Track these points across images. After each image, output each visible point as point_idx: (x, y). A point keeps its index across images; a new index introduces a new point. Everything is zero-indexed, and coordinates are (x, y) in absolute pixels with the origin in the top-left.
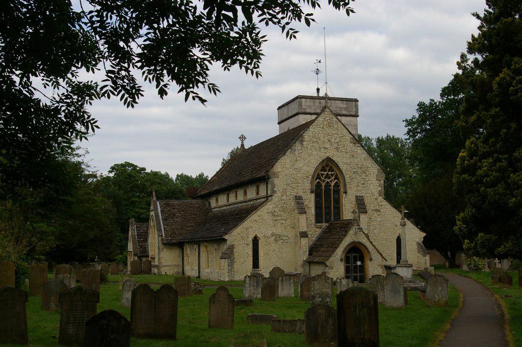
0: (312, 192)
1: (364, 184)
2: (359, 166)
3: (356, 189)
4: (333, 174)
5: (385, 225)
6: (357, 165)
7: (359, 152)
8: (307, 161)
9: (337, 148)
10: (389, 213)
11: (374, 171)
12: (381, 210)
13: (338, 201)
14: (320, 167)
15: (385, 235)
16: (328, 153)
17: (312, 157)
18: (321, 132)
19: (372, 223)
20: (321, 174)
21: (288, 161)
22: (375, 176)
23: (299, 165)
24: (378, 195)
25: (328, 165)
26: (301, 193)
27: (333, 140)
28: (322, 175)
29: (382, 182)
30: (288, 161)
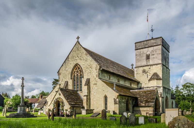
0: (71, 79)
1: (90, 73)
2: (89, 65)
3: (87, 75)
7: (89, 58)
8: (70, 67)
9: (80, 59)
10: (100, 85)
12: (97, 84)
13: (81, 82)
15: (99, 95)
16: (77, 62)
17: (71, 65)
21: (64, 68)
23: (67, 69)
24: (96, 77)
25: (77, 66)
26: (68, 80)
27: (79, 56)
28: (76, 71)
29: (98, 70)
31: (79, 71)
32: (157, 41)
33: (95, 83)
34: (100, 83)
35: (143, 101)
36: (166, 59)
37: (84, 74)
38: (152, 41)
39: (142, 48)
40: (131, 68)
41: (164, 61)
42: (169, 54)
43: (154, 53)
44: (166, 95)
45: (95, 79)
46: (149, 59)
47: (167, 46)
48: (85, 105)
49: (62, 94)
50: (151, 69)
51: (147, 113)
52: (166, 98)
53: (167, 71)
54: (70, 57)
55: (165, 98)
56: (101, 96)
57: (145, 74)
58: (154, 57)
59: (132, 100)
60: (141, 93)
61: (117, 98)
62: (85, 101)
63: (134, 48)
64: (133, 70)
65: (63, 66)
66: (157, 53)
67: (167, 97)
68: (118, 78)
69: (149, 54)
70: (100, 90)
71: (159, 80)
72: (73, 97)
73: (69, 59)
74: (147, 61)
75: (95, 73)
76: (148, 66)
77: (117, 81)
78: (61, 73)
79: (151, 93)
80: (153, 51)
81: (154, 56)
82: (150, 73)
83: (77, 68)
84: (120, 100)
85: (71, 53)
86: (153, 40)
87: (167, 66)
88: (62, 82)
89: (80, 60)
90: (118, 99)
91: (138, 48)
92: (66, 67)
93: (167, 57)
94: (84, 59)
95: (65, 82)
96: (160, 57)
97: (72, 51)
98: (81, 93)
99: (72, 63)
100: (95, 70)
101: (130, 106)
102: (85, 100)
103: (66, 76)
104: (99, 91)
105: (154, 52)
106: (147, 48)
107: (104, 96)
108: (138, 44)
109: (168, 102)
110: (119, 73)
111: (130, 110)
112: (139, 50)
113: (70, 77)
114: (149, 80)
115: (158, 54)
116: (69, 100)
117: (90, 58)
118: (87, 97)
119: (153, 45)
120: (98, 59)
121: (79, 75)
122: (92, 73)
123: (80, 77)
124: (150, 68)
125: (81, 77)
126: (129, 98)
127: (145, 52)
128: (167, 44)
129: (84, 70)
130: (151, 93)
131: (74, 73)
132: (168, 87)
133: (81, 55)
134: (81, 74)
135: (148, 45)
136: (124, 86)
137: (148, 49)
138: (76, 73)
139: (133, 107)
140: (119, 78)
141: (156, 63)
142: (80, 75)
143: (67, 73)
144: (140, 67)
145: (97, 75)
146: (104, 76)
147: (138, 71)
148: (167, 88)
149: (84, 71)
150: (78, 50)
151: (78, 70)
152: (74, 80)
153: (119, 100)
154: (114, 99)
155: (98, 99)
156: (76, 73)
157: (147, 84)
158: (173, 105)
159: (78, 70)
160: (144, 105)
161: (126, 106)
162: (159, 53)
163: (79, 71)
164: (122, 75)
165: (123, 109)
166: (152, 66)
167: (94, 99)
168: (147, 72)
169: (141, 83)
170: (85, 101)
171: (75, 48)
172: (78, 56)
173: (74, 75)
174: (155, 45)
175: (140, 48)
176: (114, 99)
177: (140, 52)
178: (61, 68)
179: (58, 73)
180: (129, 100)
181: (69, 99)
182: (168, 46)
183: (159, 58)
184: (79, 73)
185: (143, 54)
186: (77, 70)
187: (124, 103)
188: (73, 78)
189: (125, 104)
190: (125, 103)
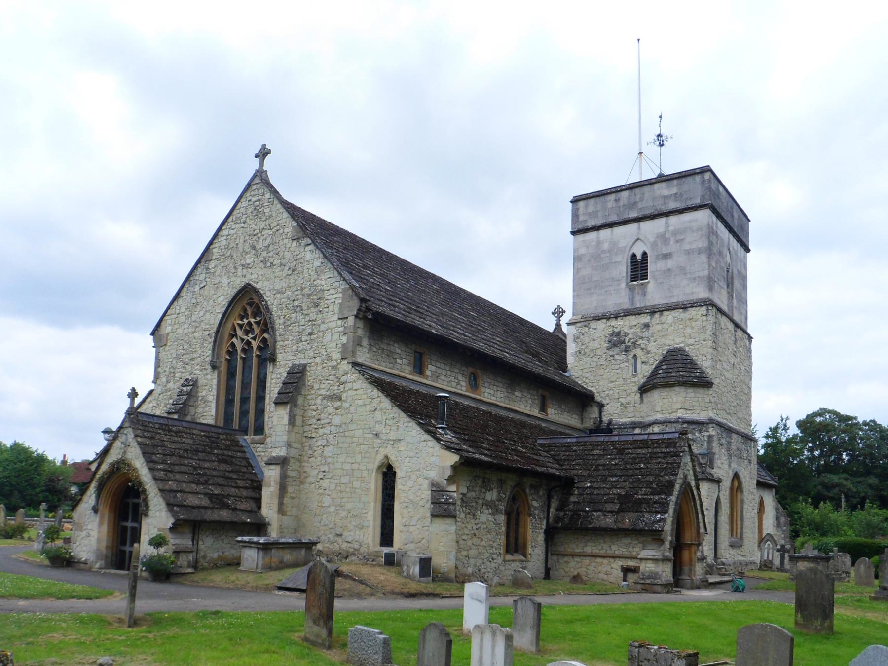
1: (310, 334)
2: (306, 291)
3: (294, 348)
4: (260, 321)
5: (351, 433)
6: (302, 289)
7: (308, 256)
10: (361, 402)
11: (335, 296)
12: (344, 396)
13: (262, 384)
14: (238, 311)
15: (350, 460)
16: (248, 276)
18: (240, 233)
19: (321, 431)
20: (238, 324)
21: (183, 310)
22: (337, 310)
24: (339, 356)
27: (259, 246)
28: (241, 326)
29: (351, 320)
30: (183, 310)
31: (258, 323)
32: (685, 187)
33: (335, 389)
34: (360, 392)
35: (606, 502)
36: (732, 278)
37: (279, 344)
38: (662, 190)
39: (610, 225)
40: (549, 325)
41: (724, 292)
42: (745, 257)
43: (672, 247)
44: (734, 465)
45: (335, 368)
46: (645, 277)
47: (736, 215)
48: (269, 510)
49: (139, 444)
50: (655, 328)
51: (626, 571)
52: (733, 480)
53: (736, 341)
54: (216, 251)
55: (726, 484)
56: (362, 467)
57: (622, 357)
58: (669, 270)
59: (541, 493)
60: (595, 452)
61: (451, 480)
62: (272, 489)
63: (567, 225)
64: (561, 336)
65: (180, 301)
66: (687, 247)
67: (736, 476)
68: (471, 370)
69: (645, 254)
70: (358, 433)
71: (693, 385)
72: (207, 465)
73: (212, 265)
74: (631, 289)
75: (336, 336)
76: (637, 312)
77: (463, 384)
78: (168, 334)
79: (653, 456)
80: (663, 238)
81: (670, 263)
82: (648, 353)
83: (248, 308)
84: (472, 494)
85: (225, 232)
86: (664, 184)
87: (736, 318)
88: (168, 382)
89: (262, 265)
90: (453, 488)
91: (591, 223)
92: (196, 305)
93: (735, 272)
94: (283, 261)
95: (182, 382)
96: (700, 266)
97: (230, 219)
98: (260, 448)
99: (225, 281)
100: (336, 318)
101: (529, 526)
102: (272, 483)
103: (193, 352)
104: (353, 437)
105: (672, 242)
106: (633, 227)
107: (380, 467)
108: (586, 206)
109: (742, 501)
110: (480, 346)
111: (530, 550)
112: (592, 235)
113: (209, 359)
114: (644, 389)
115: (688, 252)
116: (175, 480)
117: (311, 256)
118: (282, 468)
119: (665, 208)
120: (365, 267)
121: (255, 344)
122: (320, 334)
123: (257, 356)
124: (647, 326)
125: (265, 360)
126: (525, 480)
127: (622, 244)
128: (735, 207)
129: (282, 321)
130: (653, 456)
131: (232, 336)
132: (741, 428)
133: (269, 239)
134: (265, 341)
135: (640, 205)
136: (502, 413)
137: (639, 228)
138: (240, 333)
139: (550, 534)
140: (479, 372)
141: (679, 297)
142: (259, 348)
143: (196, 335)
144: (598, 318)
145: (343, 345)
146: (390, 354)
147: (586, 340)
148: (738, 433)
149: (279, 323)
150: (257, 211)
151: (252, 320)
152: (231, 374)
153: (464, 491)
154: (434, 485)
155: (345, 480)
156: (240, 333)
157: (630, 409)
158: (764, 516)
159: (252, 320)
160: (609, 521)
161: (503, 529)
162: (694, 246)
163: (254, 326)
164: (498, 354)
165: (484, 543)
166: (657, 315)
167: (325, 483)
168: (634, 343)
169: (598, 398)
170: (272, 489)
171: (244, 203)
172: (254, 248)
173: (233, 345)
174: (673, 205)
175: (599, 222)
176: (434, 485)
177: (599, 243)
178: (168, 308)
179: (153, 334)
180: (524, 491)
181: (178, 476)
182: (742, 216)
183: (696, 275)
184: (254, 338)
185: (610, 251)
186: (246, 321)
187: (496, 511)
188: (223, 360)
189: (502, 518)
190: (502, 507)
